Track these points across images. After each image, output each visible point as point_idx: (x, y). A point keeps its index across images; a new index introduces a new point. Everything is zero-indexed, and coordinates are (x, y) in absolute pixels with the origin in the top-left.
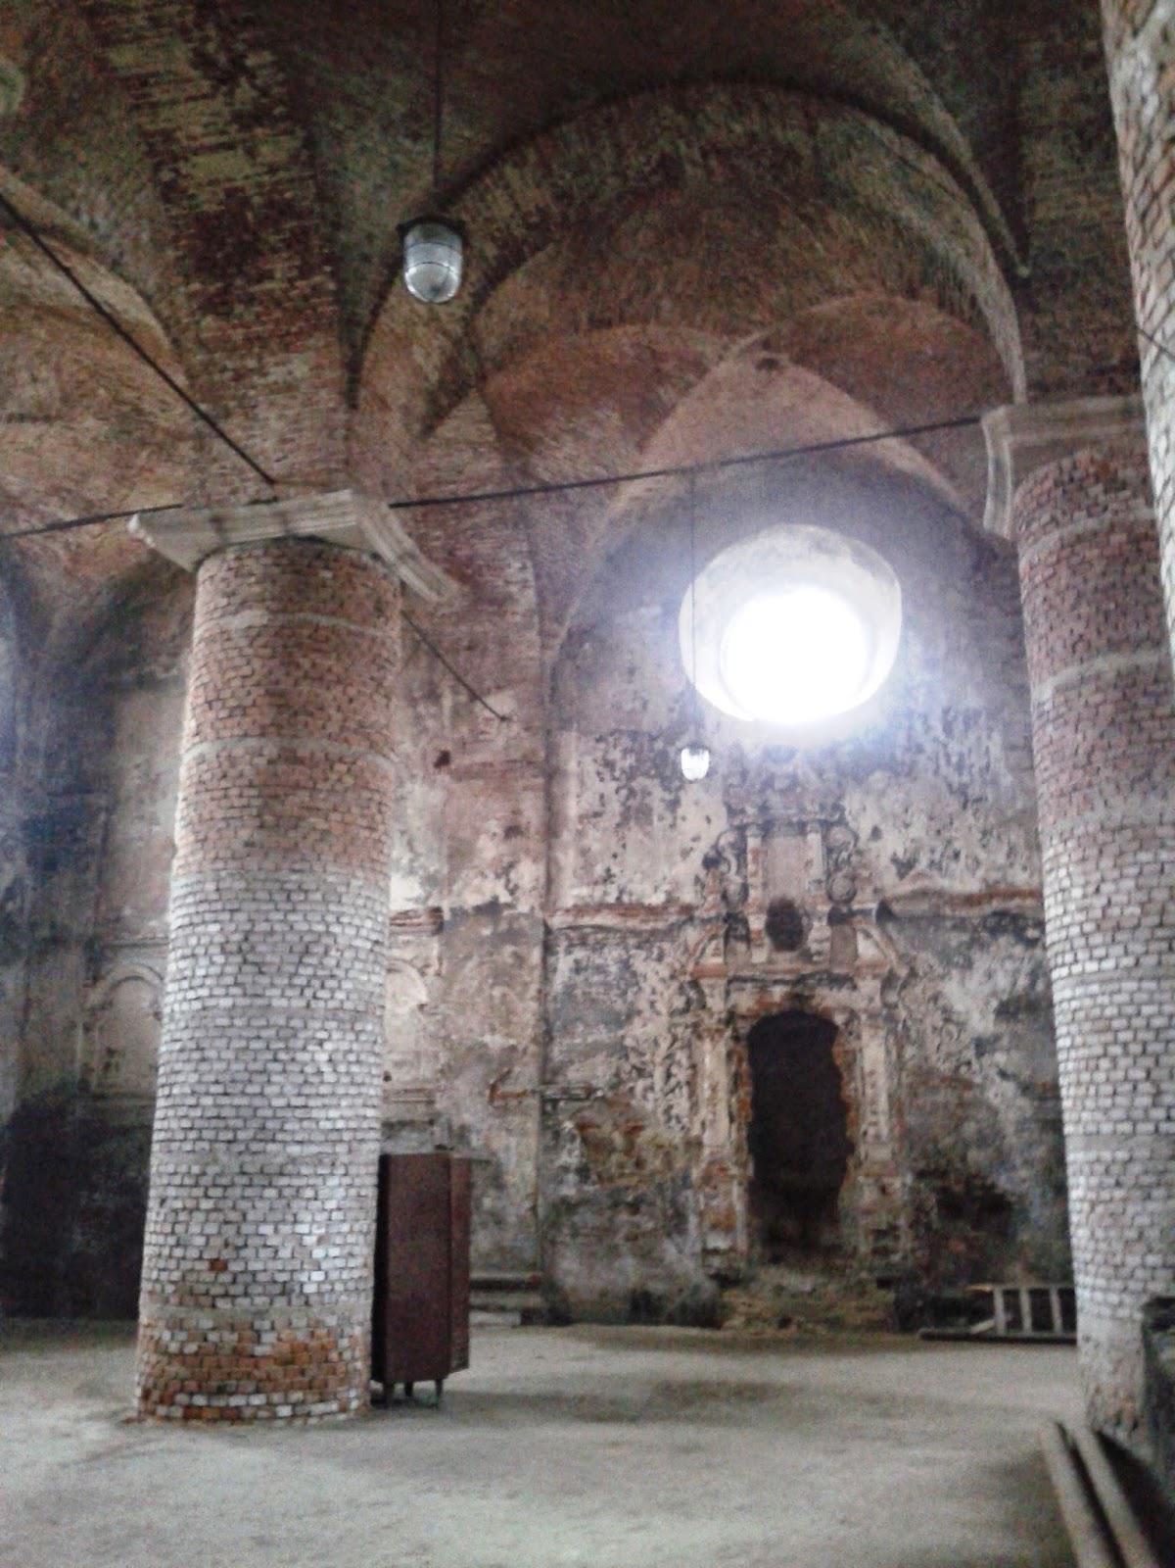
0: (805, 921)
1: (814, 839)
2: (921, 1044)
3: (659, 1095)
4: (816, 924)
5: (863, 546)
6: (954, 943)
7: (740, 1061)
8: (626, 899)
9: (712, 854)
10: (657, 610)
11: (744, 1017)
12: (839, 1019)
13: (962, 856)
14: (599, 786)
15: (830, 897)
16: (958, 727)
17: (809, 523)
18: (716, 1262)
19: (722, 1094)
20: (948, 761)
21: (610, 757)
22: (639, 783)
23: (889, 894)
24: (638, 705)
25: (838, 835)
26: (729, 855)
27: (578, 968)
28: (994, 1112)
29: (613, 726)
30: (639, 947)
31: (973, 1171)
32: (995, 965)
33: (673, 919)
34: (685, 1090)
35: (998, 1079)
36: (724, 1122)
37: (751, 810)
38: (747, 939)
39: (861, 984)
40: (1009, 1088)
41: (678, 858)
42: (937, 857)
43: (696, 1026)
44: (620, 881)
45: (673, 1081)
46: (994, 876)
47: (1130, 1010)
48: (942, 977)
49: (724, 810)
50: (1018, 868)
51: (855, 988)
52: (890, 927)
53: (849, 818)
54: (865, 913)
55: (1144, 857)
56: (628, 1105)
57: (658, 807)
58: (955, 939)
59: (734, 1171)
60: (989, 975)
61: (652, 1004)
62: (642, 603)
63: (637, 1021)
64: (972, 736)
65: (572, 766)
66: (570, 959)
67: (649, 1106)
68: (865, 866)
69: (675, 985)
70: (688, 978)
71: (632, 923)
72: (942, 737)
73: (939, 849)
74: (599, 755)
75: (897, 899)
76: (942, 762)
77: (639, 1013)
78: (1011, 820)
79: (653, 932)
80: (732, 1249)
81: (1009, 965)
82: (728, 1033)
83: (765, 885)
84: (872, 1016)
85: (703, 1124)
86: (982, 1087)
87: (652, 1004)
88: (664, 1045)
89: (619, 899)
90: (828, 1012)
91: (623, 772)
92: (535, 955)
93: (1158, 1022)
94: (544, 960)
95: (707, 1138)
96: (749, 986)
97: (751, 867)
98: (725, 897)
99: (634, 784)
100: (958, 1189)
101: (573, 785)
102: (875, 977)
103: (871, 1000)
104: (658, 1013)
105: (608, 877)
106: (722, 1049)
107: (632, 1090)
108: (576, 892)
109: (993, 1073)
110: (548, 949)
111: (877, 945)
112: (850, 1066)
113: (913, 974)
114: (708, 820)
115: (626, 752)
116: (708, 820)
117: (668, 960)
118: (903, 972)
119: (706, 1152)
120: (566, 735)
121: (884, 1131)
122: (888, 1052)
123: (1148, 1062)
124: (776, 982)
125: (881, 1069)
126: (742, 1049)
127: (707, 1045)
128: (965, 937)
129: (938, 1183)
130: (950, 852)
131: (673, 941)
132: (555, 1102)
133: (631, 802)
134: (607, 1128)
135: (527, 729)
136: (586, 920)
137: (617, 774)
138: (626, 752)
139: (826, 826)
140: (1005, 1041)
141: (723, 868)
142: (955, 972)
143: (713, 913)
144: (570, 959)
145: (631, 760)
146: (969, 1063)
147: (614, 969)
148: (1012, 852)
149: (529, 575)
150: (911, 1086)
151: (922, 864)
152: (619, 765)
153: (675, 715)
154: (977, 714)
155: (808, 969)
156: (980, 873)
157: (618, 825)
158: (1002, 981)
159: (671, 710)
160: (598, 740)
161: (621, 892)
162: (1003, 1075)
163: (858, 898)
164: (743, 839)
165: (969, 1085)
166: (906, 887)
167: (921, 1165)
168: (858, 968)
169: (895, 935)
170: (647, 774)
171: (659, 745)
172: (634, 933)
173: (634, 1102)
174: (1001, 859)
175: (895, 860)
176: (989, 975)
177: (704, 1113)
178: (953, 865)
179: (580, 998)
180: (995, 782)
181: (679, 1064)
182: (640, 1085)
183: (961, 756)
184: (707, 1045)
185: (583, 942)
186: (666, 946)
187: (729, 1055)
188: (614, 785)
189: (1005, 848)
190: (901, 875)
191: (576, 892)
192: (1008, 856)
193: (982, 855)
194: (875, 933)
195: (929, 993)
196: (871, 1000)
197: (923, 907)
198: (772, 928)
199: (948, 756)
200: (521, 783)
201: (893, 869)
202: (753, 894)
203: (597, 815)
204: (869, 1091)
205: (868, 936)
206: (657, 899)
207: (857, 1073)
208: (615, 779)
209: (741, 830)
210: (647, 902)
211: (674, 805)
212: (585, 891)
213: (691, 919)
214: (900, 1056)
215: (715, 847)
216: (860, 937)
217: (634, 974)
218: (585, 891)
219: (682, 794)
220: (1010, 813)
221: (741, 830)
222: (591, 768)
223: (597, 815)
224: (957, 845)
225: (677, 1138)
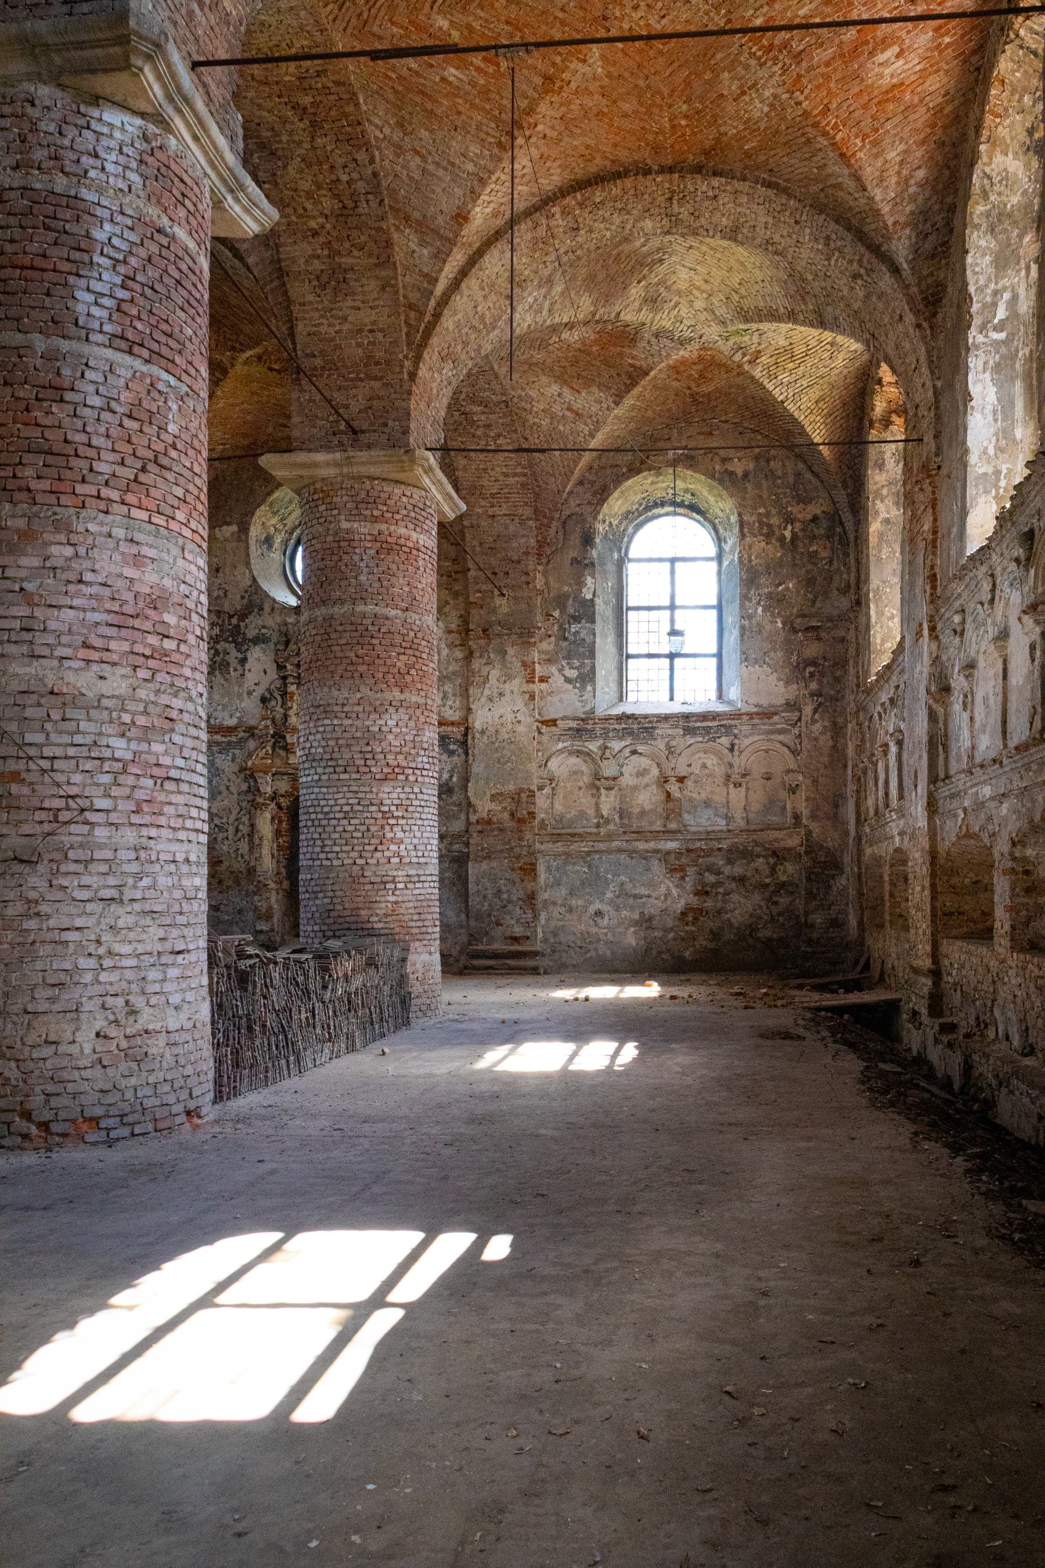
7: (280, 822)
47: (315, 803)
50: (447, 708)
55: (327, 722)
80: (272, 930)
93: (326, 809)
123: (320, 830)
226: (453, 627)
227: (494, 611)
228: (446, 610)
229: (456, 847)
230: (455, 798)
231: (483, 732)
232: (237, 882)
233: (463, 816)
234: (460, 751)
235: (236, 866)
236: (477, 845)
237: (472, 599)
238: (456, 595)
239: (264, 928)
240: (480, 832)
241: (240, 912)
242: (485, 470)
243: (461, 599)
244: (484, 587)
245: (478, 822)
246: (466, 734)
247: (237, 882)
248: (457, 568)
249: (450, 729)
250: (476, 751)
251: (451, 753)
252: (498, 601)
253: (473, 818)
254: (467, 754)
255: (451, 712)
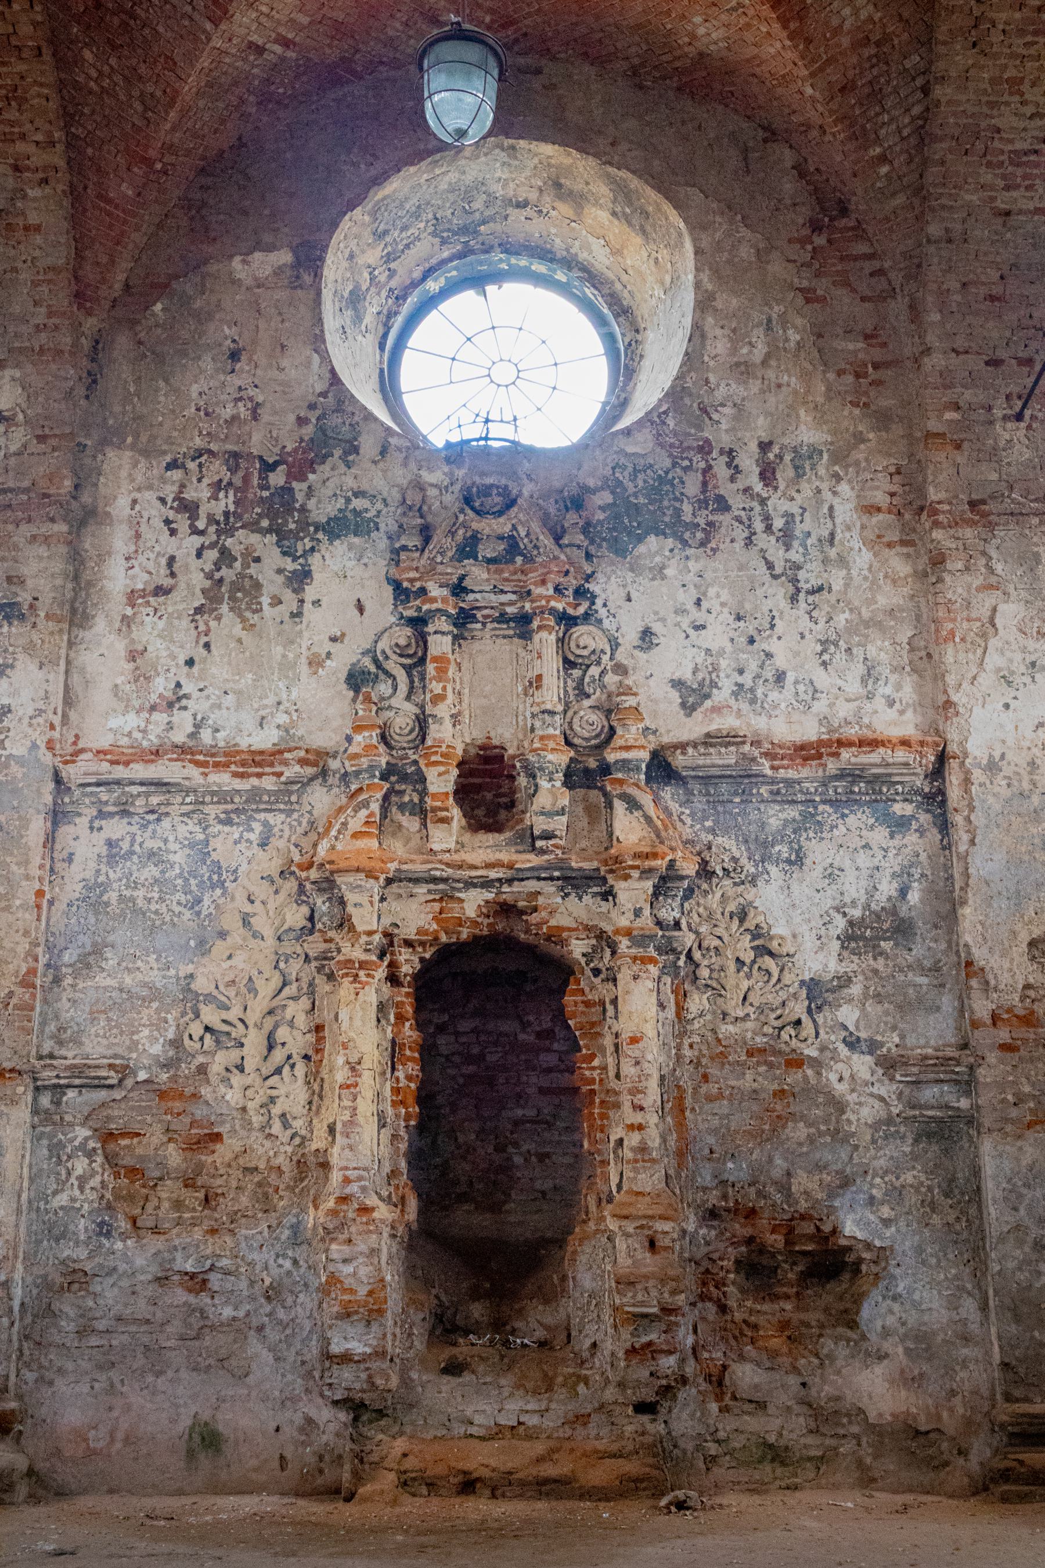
0: (522, 781)
1: (546, 640)
2: (717, 991)
3: (252, 1078)
4: (544, 784)
5: (635, 183)
6: (774, 823)
7: (400, 1018)
8: (206, 737)
9: (367, 663)
10: (284, 257)
11: (408, 943)
12: (578, 948)
13: (790, 677)
14: (170, 545)
15: (568, 743)
16: (785, 474)
17: (543, 139)
18: (347, 1377)
19: (368, 1082)
20: (769, 528)
21: (189, 495)
22: (238, 542)
23: (666, 740)
24: (243, 410)
25: (585, 637)
26: (393, 665)
27: (113, 852)
28: (840, 1106)
29: (198, 443)
30: (228, 822)
31: (803, 1205)
32: (841, 859)
33: (289, 773)
34: (300, 1069)
35: (843, 1050)
36: (368, 1129)
37: (435, 591)
38: (421, 812)
39: (621, 888)
40: (862, 1065)
41: (304, 669)
42: (747, 680)
43: (324, 957)
44: (197, 705)
45: (278, 1056)
46: (844, 710)
48: (753, 881)
49: (388, 591)
50: (879, 703)
51: (608, 895)
52: (667, 793)
53: (603, 612)
54: (625, 765)
56: (195, 1096)
57: (271, 582)
58: (776, 817)
59: (383, 1212)
60: (832, 874)
61: (246, 921)
62: (259, 246)
63: (220, 948)
64: (807, 490)
65: (121, 506)
66: (100, 838)
67: (233, 1097)
68: (629, 692)
69: (290, 886)
70: (314, 874)
71: (222, 779)
72: (758, 487)
73: (753, 666)
74: (170, 491)
75: (683, 746)
76: (759, 526)
77: (223, 935)
78: (867, 624)
79: (255, 795)
80: (380, 1354)
81: (864, 860)
82: (381, 973)
83: (456, 718)
84: (640, 940)
85: (332, 1130)
86: (817, 1064)
87: (246, 921)
88: (266, 989)
89: (193, 735)
90: (556, 936)
91: (211, 520)
92: (37, 827)
94: (50, 840)
95: (336, 1157)
96: (421, 890)
97: (436, 687)
98: (384, 738)
99: (229, 543)
100: (776, 1240)
101: (120, 541)
102: (645, 873)
103: (638, 912)
104: (257, 935)
105: (176, 700)
106: (371, 997)
107: (202, 1069)
108: (114, 723)
109: (836, 1040)
110: (57, 816)
111: (648, 819)
112: (593, 1029)
113: (706, 872)
114: (361, 608)
115: (218, 486)
116: (361, 608)
117: (276, 843)
118: (689, 868)
119: (336, 1177)
120: (111, 453)
121: (653, 1137)
122: (662, 1006)
124: (470, 884)
125: (650, 1031)
126: (404, 996)
127: (346, 987)
128: (792, 813)
129: (740, 1229)
130: (769, 674)
131: (289, 813)
132: (58, 1090)
133: (224, 572)
134: (155, 1136)
135: (41, 439)
136: (140, 771)
137: (201, 525)
138: (218, 486)
139: (567, 621)
140: (856, 990)
141: (384, 688)
142: (773, 870)
143: (365, 762)
144: (100, 838)
145: (227, 501)
146: (798, 1022)
147: (179, 857)
148: (869, 675)
149: (57, 157)
150: (697, 1063)
151: (722, 695)
152: (203, 512)
153: (308, 431)
154: (815, 452)
155: (532, 860)
156: (820, 706)
157: (199, 610)
158: (853, 888)
159: (301, 421)
160: (169, 467)
161: (197, 726)
162: (852, 1043)
163: (617, 742)
164: (422, 639)
165: (796, 1062)
166: (693, 728)
167: (713, 1198)
168: (617, 860)
169: (674, 807)
170: (253, 527)
171: (277, 478)
172: (222, 797)
173: (205, 1091)
174: (854, 687)
175: (678, 684)
176: (832, 874)
177: (334, 1111)
178: (774, 695)
179: (114, 908)
180: (842, 561)
181: (291, 1024)
182: (221, 1060)
183: (789, 517)
184: (346, 987)
185: (125, 813)
186: (276, 820)
187: (381, 1007)
188: (197, 541)
189: (860, 669)
190: (689, 709)
191: (114, 723)
192: (864, 681)
193: (822, 679)
194: (646, 799)
195: (732, 907)
196: (638, 912)
197: (727, 757)
198: (463, 793)
199: (767, 518)
200: (26, 530)
201: (675, 696)
202: (435, 732)
203: (160, 591)
204: (628, 1069)
205: (633, 805)
206: (265, 739)
207: (608, 1041)
208: (196, 532)
209: (418, 623)
210: (244, 743)
211: (300, 579)
212: (132, 721)
213: (324, 773)
214: (680, 1009)
215: (371, 652)
216: (619, 806)
217: (217, 867)
218: (132, 721)
219: (315, 561)
220: (866, 614)
221: (418, 623)
222: (155, 512)
223: (160, 591)
224: (781, 661)
225: (283, 1155)
226: (880, 498)
227: (993, 455)
228: (859, 454)
229: (929, 1094)
230: (918, 950)
231: (992, 767)
232: (265, 1202)
233: (947, 1002)
234: (924, 818)
235: (261, 1150)
236: (1001, 1086)
237: (933, 425)
238: (883, 420)
239: (358, 1348)
240: (1006, 1048)
241: (272, 1294)
242: (1015, 83)
243: (898, 430)
244: (968, 395)
245: (995, 1018)
246: (938, 771)
247: (265, 1202)
248: (877, 354)
249: (901, 755)
250: (978, 819)
251: (901, 825)
252: (1006, 432)
253: (982, 1007)
254: (944, 826)
255: (892, 714)
